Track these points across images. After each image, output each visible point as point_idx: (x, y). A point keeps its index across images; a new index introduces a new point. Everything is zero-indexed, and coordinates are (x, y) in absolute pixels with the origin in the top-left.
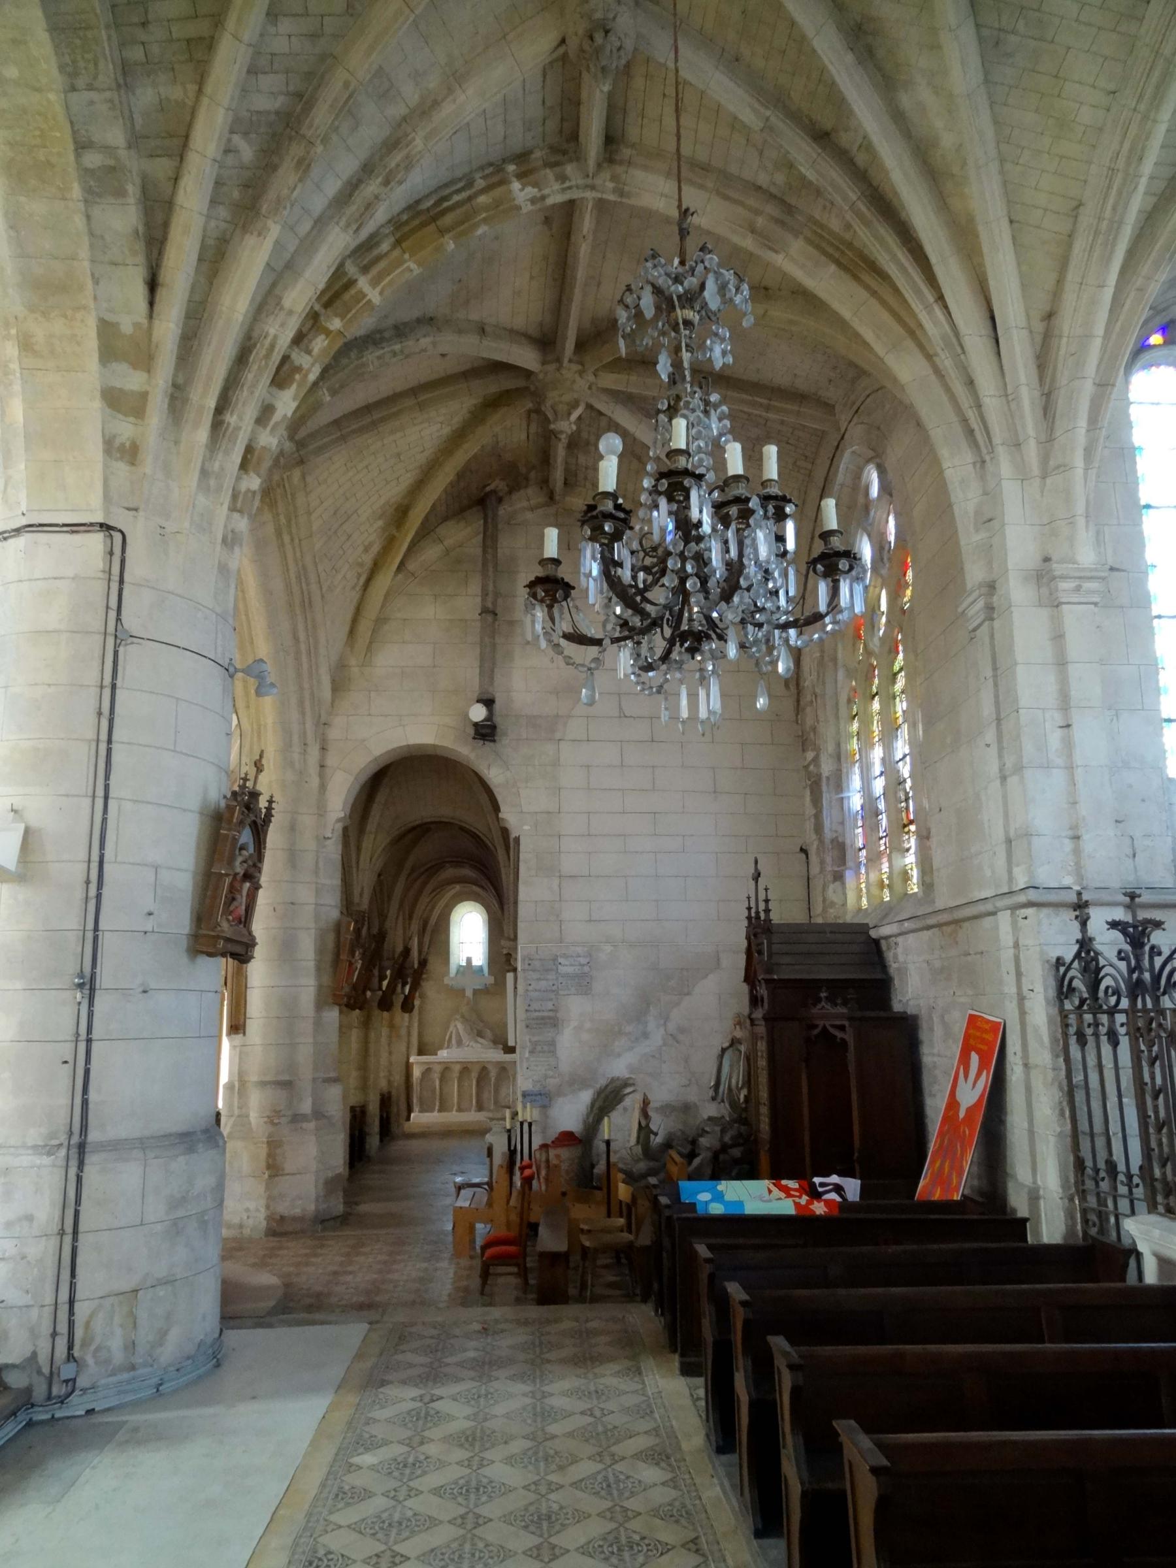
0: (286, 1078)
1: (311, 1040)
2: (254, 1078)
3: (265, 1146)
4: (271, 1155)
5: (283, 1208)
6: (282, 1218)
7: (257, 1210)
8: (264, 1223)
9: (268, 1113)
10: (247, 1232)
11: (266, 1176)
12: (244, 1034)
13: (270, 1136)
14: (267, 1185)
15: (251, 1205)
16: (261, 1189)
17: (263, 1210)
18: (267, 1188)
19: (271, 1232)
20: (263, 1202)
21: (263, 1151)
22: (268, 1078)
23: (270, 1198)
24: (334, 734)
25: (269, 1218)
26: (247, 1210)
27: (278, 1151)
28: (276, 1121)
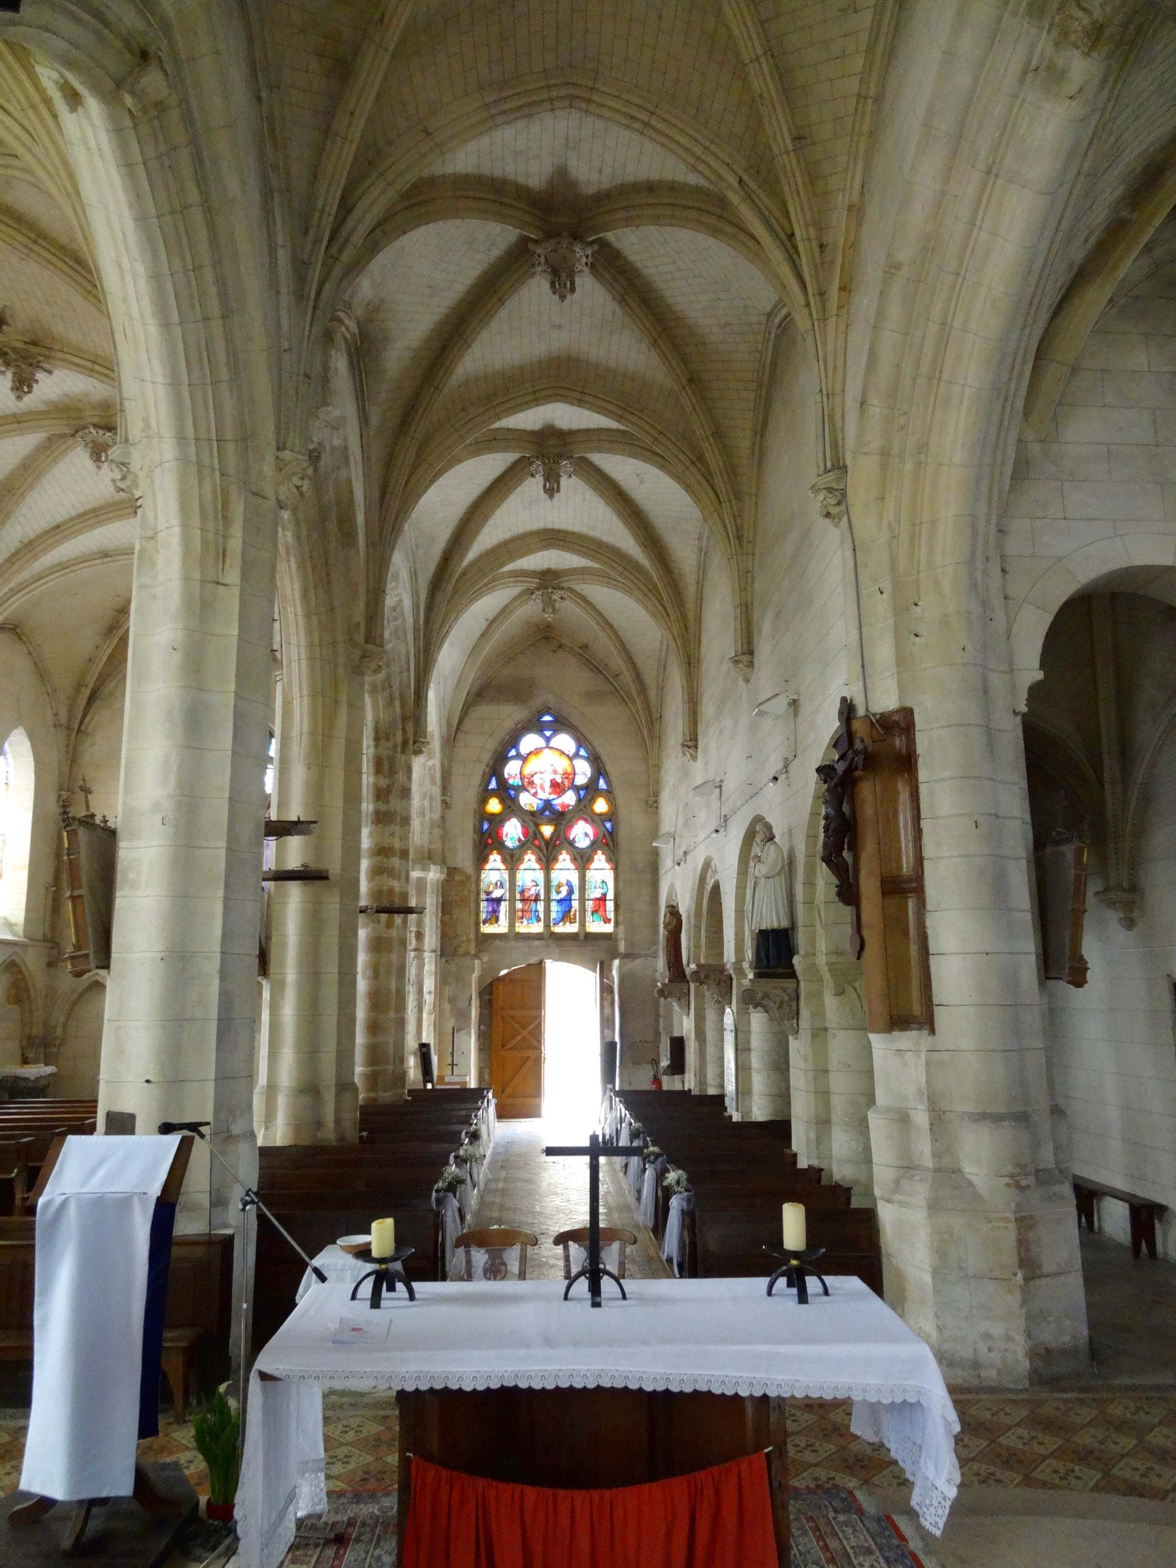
0: (1021, 1109)
1: (1041, 1046)
2: (961, 1102)
3: (1012, 1226)
4: (1022, 1243)
5: (1049, 1335)
6: (1048, 1351)
7: (1009, 1338)
8: (1026, 1365)
9: (1009, 1168)
10: (990, 1375)
11: (1020, 1277)
12: (932, 1031)
13: (1019, 1207)
14: (1023, 1291)
15: (997, 1330)
16: (1013, 1300)
17: (1020, 1338)
18: (1024, 1302)
19: (1038, 1378)
20: (1021, 1323)
21: (1009, 1236)
22: (999, 1108)
23: (1034, 1318)
24: (1013, 546)
25: (1033, 1354)
26: (987, 1336)
27: (1031, 1235)
28: (1023, 1183)
